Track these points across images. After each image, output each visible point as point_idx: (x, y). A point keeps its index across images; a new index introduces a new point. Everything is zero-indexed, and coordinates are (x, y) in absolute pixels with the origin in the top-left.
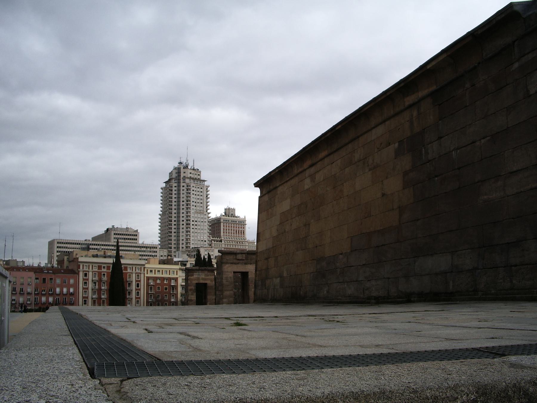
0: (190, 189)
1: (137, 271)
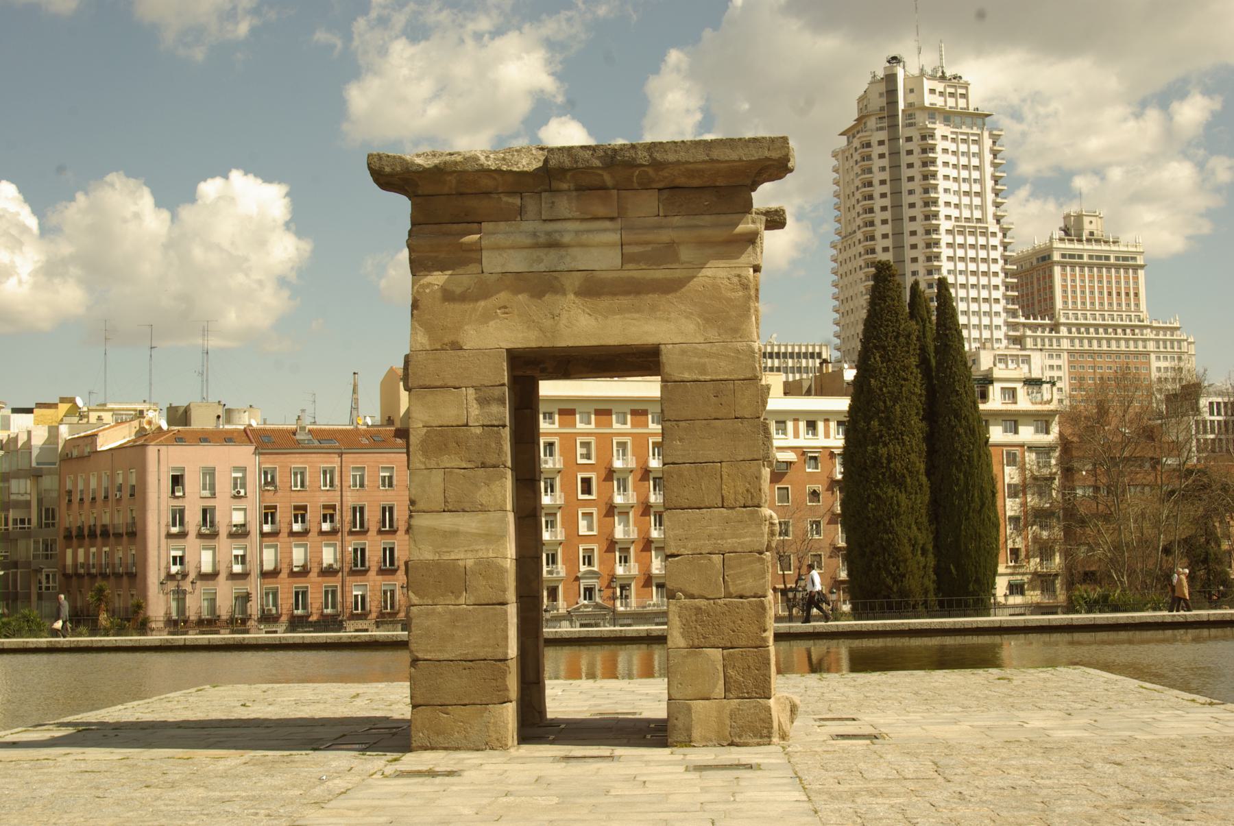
0: (933, 149)
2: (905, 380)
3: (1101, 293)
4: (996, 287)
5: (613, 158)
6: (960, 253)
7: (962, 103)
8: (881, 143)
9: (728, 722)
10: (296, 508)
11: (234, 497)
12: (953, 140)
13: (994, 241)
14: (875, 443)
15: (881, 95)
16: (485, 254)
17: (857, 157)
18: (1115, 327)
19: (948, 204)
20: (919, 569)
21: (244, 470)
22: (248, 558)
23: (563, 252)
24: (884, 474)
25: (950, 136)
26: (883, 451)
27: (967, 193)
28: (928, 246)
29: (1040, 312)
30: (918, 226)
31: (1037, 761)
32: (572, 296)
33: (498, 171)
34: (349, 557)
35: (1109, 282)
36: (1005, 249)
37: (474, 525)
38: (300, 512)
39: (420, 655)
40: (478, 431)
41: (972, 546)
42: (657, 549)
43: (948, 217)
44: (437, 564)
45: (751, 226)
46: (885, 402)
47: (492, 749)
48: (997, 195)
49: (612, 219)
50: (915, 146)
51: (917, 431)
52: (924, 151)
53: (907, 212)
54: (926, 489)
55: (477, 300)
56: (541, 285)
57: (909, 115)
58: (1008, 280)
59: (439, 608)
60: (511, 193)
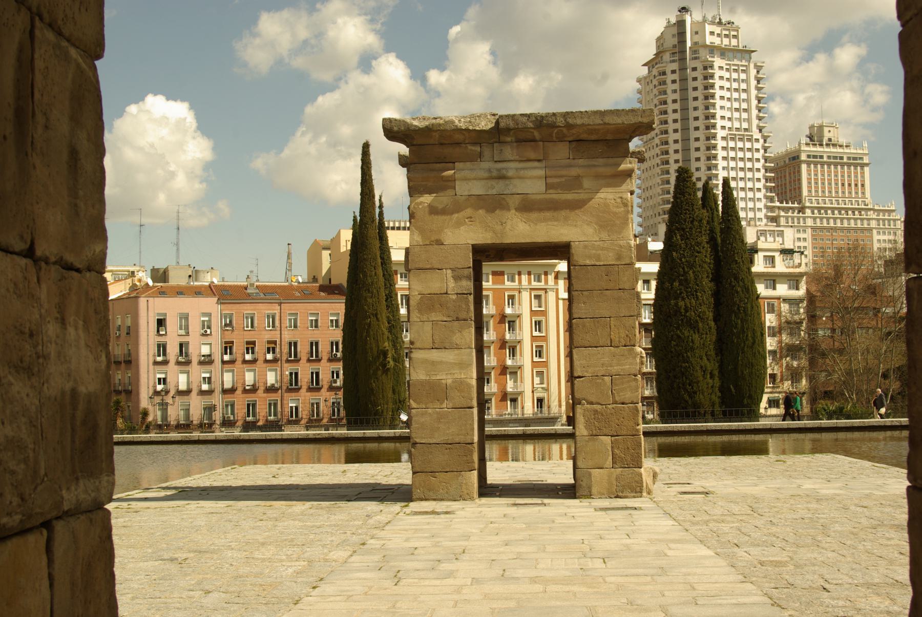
0: (712, 76)
1: (535, 284)
2: (698, 252)
3: (837, 184)
4: (759, 180)
5: (541, 121)
6: (732, 154)
7: (734, 42)
8: (673, 72)
9: (614, 483)
10: (248, 343)
11: (203, 335)
12: (727, 70)
13: (757, 146)
14: (676, 298)
15: (674, 36)
16: (457, 183)
17: (655, 82)
18: (847, 210)
19: (723, 118)
20: (708, 388)
21: (209, 315)
22: (213, 380)
23: (507, 182)
24: (682, 320)
25: (725, 67)
26: (681, 304)
27: (737, 110)
28: (708, 149)
29: (791, 198)
30: (701, 134)
31: (814, 505)
32: (513, 211)
33: (467, 130)
34: (286, 379)
35: (843, 176)
36: (765, 151)
37: (451, 357)
38: (250, 346)
39: (418, 441)
40: (454, 297)
41: (746, 372)
42: (511, 373)
43: (723, 128)
44: (428, 382)
45: (629, 166)
46: (683, 268)
47: (464, 500)
48: (759, 111)
49: (539, 161)
50: (699, 74)
51: (707, 289)
52: (706, 78)
53: (693, 124)
54: (714, 331)
55: (452, 214)
56: (493, 204)
57: (694, 51)
58: (768, 174)
59: (430, 411)
60: (475, 144)
